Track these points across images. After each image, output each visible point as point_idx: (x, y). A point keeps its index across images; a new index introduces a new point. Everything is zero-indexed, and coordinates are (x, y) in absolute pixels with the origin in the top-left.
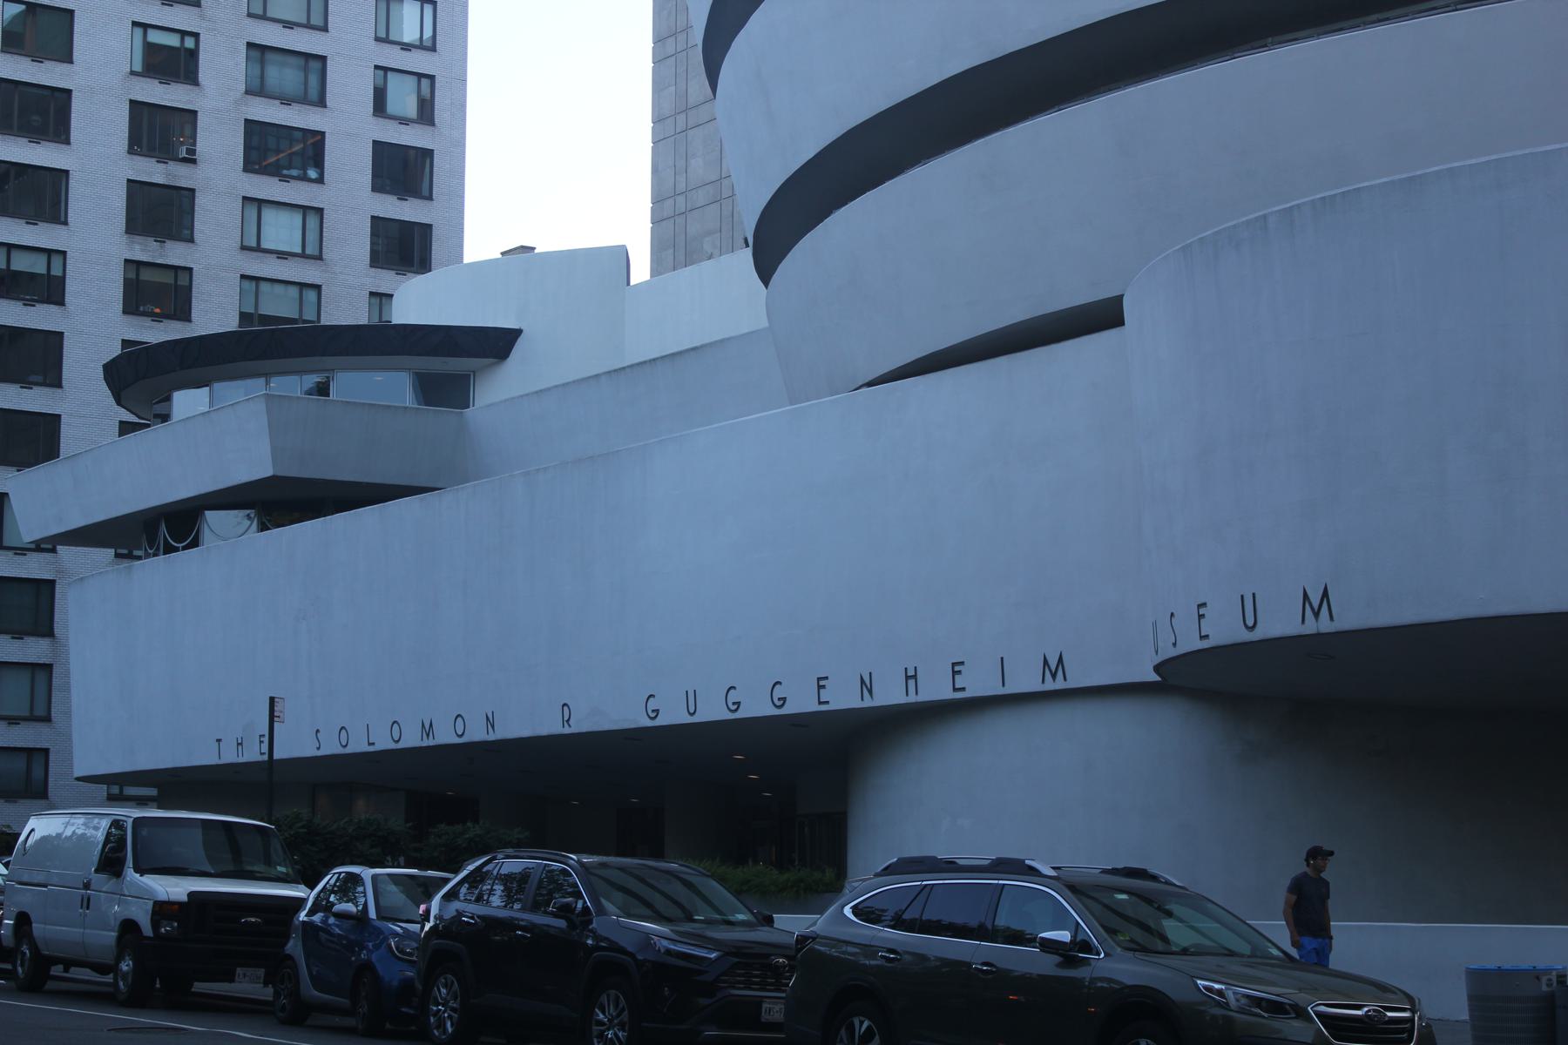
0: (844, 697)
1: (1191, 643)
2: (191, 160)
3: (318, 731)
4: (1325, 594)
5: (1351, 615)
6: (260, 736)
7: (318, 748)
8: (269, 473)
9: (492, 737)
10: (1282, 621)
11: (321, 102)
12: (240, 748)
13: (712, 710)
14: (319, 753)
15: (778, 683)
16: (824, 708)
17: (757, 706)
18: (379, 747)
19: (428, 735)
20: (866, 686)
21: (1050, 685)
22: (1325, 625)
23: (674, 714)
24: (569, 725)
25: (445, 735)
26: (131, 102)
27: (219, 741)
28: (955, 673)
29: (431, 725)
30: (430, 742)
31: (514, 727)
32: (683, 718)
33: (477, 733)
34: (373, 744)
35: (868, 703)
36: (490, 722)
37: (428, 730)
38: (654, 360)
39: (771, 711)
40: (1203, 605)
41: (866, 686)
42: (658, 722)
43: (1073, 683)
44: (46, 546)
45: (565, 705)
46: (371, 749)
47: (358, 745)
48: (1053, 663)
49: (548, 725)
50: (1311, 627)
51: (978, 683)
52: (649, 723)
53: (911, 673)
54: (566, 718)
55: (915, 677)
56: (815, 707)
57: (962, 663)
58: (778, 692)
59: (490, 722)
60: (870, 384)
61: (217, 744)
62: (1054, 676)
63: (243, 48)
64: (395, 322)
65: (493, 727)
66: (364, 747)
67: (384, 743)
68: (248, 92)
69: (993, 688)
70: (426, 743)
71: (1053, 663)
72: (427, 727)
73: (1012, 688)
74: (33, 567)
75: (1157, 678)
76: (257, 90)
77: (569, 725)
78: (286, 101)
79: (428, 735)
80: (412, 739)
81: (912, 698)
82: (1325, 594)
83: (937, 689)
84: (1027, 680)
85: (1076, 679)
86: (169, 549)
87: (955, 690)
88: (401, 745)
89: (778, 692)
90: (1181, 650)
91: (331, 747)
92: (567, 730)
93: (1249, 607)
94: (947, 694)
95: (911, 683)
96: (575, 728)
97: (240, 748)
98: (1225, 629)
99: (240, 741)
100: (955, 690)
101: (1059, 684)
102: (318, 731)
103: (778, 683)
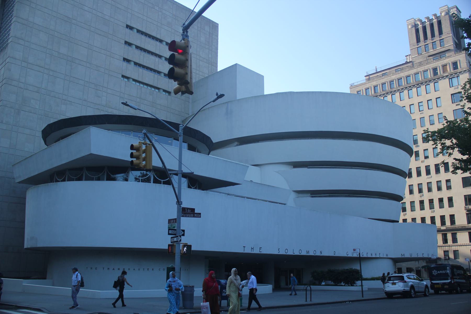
3: (279, 249)
6: (260, 248)
7: (279, 253)
9: (321, 255)
12: (252, 250)
18: (296, 254)
19: (308, 253)
20: (372, 255)
25: (311, 254)
27: (244, 247)
29: (309, 251)
30: (308, 254)
33: (318, 254)
34: (294, 253)
35: (371, 257)
36: (321, 253)
37: (308, 252)
38: (265, 185)
41: (372, 255)
42: (348, 256)
45: (315, 250)
47: (290, 253)
49: (332, 254)
52: (347, 256)
59: (321, 253)
65: (321, 253)
66: (292, 254)
67: (297, 253)
70: (307, 254)
72: (308, 251)
79: (308, 253)
80: (304, 253)
81: (376, 257)
84: (385, 256)
85: (389, 257)
88: (287, 254)
89: (363, 254)
90: (418, 257)
91: (282, 252)
92: (335, 256)
96: (336, 255)
97: (252, 250)
99: (252, 248)
101: (387, 257)
102: (279, 249)
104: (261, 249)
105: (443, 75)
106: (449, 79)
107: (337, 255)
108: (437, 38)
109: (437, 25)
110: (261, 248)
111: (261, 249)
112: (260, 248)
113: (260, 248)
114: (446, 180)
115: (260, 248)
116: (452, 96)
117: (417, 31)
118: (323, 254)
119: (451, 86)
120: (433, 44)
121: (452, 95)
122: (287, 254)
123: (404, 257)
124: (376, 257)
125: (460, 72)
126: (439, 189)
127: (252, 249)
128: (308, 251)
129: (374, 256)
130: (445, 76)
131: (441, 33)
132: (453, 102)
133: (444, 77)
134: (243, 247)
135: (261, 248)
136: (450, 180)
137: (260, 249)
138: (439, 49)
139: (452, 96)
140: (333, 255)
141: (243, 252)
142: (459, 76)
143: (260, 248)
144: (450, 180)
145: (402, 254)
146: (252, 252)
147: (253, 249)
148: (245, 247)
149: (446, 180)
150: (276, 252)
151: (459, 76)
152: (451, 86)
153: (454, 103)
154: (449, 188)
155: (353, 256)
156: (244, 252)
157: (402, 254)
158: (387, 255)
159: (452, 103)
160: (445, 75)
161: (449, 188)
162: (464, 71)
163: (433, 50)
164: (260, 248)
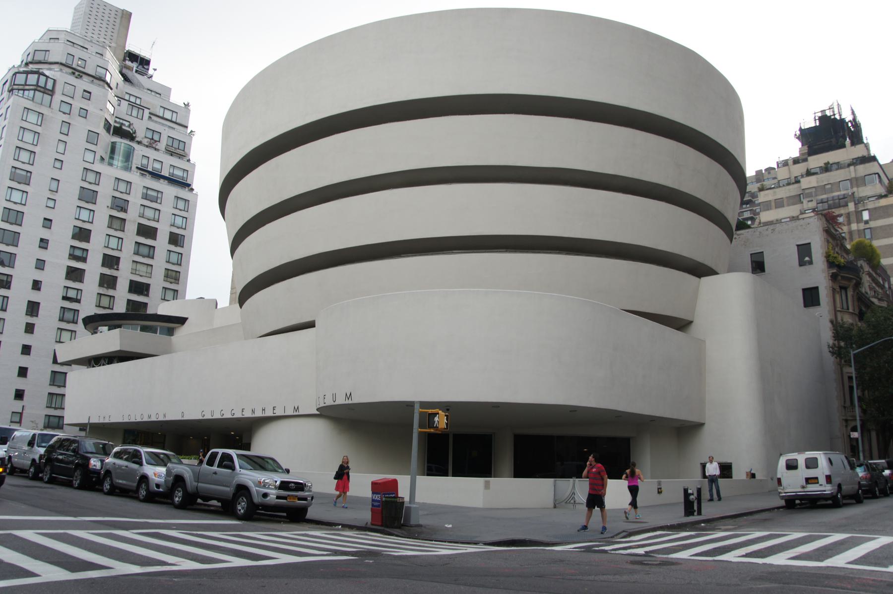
0: (248, 414)
1: (322, 405)
2: (117, 269)
4: (351, 394)
5: (356, 400)
8: (118, 349)
10: (341, 400)
11: (153, 258)
13: (217, 416)
15: (233, 410)
16: (243, 416)
17: (228, 415)
20: (253, 411)
21: (296, 413)
22: (350, 402)
23: (208, 416)
25: (154, 419)
26: (104, 254)
28: (274, 409)
31: (169, 418)
32: (210, 417)
33: (161, 418)
34: (136, 420)
35: (253, 416)
36: (165, 416)
37: (150, 417)
39: (220, 417)
40: (325, 395)
41: (253, 411)
43: (300, 413)
44: (69, 363)
47: (133, 420)
48: (296, 408)
49: (179, 418)
50: (347, 402)
51: (279, 412)
53: (264, 409)
56: (241, 416)
57: (275, 407)
58: (233, 412)
59: (165, 416)
60: (260, 337)
62: (296, 411)
63: (134, 243)
64: (158, 313)
66: (134, 420)
67: (139, 420)
68: (134, 254)
69: (282, 414)
71: (296, 408)
73: (287, 414)
74: (63, 369)
75: (318, 413)
76: (137, 253)
78: (144, 256)
81: (264, 415)
82: (351, 394)
83: (269, 413)
84: (290, 412)
85: (302, 412)
86: (93, 367)
87: (273, 413)
89: (233, 412)
90: (320, 406)
91: (126, 420)
92: (183, 419)
93: (334, 396)
94: (272, 415)
95: (264, 411)
98: (329, 402)
100: (273, 413)
101: (297, 413)
103: (233, 410)
107: (186, 418)
118: (168, 418)
124: (265, 415)
150: (120, 420)
155: (213, 418)
158: (297, 409)
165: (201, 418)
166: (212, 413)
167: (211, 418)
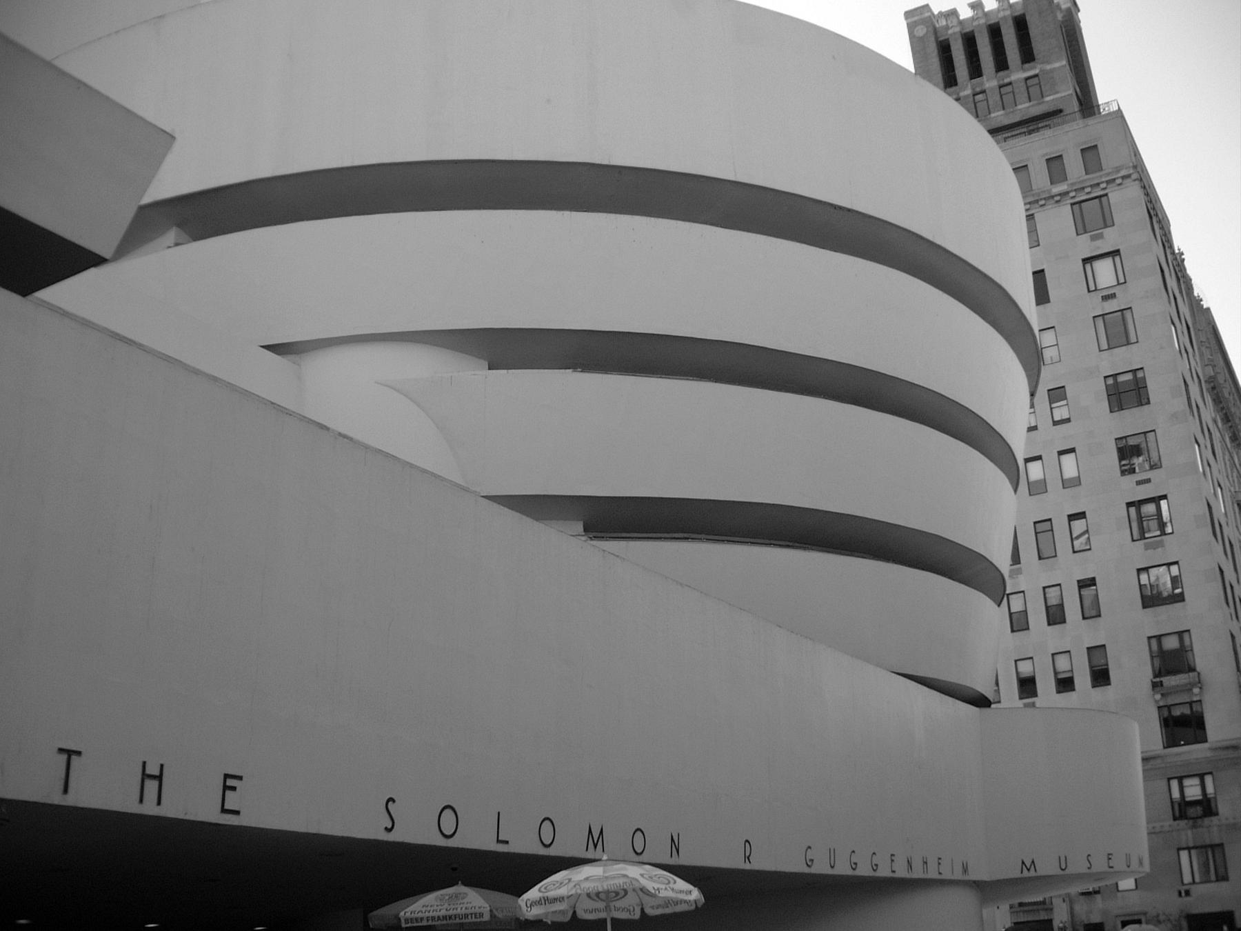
6: (227, 776)
7: (389, 830)
12: (151, 786)
14: (391, 837)
19: (595, 846)
24: (750, 862)
27: (70, 753)
32: (827, 870)
46: (501, 848)
54: (747, 854)
55: (926, 863)
61: (65, 757)
66: (487, 843)
72: (596, 834)
77: (750, 862)
79: (595, 846)
85: (973, 876)
92: (747, 867)
99: (153, 770)
101: (966, 878)
104: (234, 789)
105: (1049, 191)
106: (1072, 204)
108: (1017, 75)
109: (1013, 27)
110: (240, 778)
111: (234, 789)
112: (230, 782)
113: (227, 776)
114: (1079, 581)
115: (229, 783)
116: (1088, 267)
117: (944, 49)
119: (1082, 227)
120: (1002, 93)
121: (1086, 261)
122: (451, 843)
123: (1032, 873)
125: (1108, 182)
126: (1056, 616)
127: (145, 776)
128: (596, 834)
129: (918, 873)
130: (1056, 195)
131: (1028, 56)
132: (1092, 288)
133: (1053, 197)
134: (61, 750)
135: (240, 778)
136: (1094, 579)
137: (226, 788)
138: (1025, 108)
139: (1088, 267)
140: (738, 863)
141: (57, 799)
142: (1106, 195)
143: (229, 783)
144: (1094, 579)
145: (1023, 863)
146: (149, 808)
147: (159, 778)
148: (79, 753)
149: (1079, 581)
151: (1106, 195)
152: (1081, 231)
153: (1096, 290)
154: (1091, 612)
156: (71, 800)
157: (1023, 863)
159: (1089, 291)
160: (1057, 189)
161: (1091, 612)
162: (1123, 178)
163: (1002, 112)
164: (230, 782)
165: (801, 868)
166: (832, 853)
167: (830, 872)
